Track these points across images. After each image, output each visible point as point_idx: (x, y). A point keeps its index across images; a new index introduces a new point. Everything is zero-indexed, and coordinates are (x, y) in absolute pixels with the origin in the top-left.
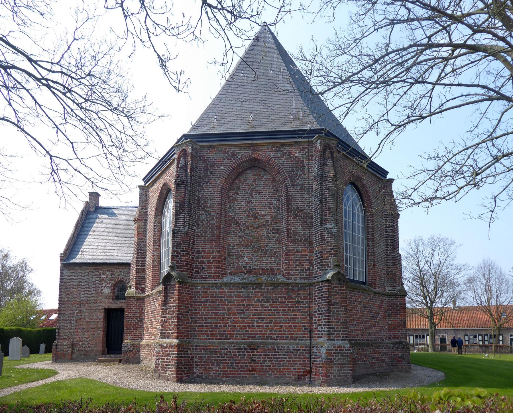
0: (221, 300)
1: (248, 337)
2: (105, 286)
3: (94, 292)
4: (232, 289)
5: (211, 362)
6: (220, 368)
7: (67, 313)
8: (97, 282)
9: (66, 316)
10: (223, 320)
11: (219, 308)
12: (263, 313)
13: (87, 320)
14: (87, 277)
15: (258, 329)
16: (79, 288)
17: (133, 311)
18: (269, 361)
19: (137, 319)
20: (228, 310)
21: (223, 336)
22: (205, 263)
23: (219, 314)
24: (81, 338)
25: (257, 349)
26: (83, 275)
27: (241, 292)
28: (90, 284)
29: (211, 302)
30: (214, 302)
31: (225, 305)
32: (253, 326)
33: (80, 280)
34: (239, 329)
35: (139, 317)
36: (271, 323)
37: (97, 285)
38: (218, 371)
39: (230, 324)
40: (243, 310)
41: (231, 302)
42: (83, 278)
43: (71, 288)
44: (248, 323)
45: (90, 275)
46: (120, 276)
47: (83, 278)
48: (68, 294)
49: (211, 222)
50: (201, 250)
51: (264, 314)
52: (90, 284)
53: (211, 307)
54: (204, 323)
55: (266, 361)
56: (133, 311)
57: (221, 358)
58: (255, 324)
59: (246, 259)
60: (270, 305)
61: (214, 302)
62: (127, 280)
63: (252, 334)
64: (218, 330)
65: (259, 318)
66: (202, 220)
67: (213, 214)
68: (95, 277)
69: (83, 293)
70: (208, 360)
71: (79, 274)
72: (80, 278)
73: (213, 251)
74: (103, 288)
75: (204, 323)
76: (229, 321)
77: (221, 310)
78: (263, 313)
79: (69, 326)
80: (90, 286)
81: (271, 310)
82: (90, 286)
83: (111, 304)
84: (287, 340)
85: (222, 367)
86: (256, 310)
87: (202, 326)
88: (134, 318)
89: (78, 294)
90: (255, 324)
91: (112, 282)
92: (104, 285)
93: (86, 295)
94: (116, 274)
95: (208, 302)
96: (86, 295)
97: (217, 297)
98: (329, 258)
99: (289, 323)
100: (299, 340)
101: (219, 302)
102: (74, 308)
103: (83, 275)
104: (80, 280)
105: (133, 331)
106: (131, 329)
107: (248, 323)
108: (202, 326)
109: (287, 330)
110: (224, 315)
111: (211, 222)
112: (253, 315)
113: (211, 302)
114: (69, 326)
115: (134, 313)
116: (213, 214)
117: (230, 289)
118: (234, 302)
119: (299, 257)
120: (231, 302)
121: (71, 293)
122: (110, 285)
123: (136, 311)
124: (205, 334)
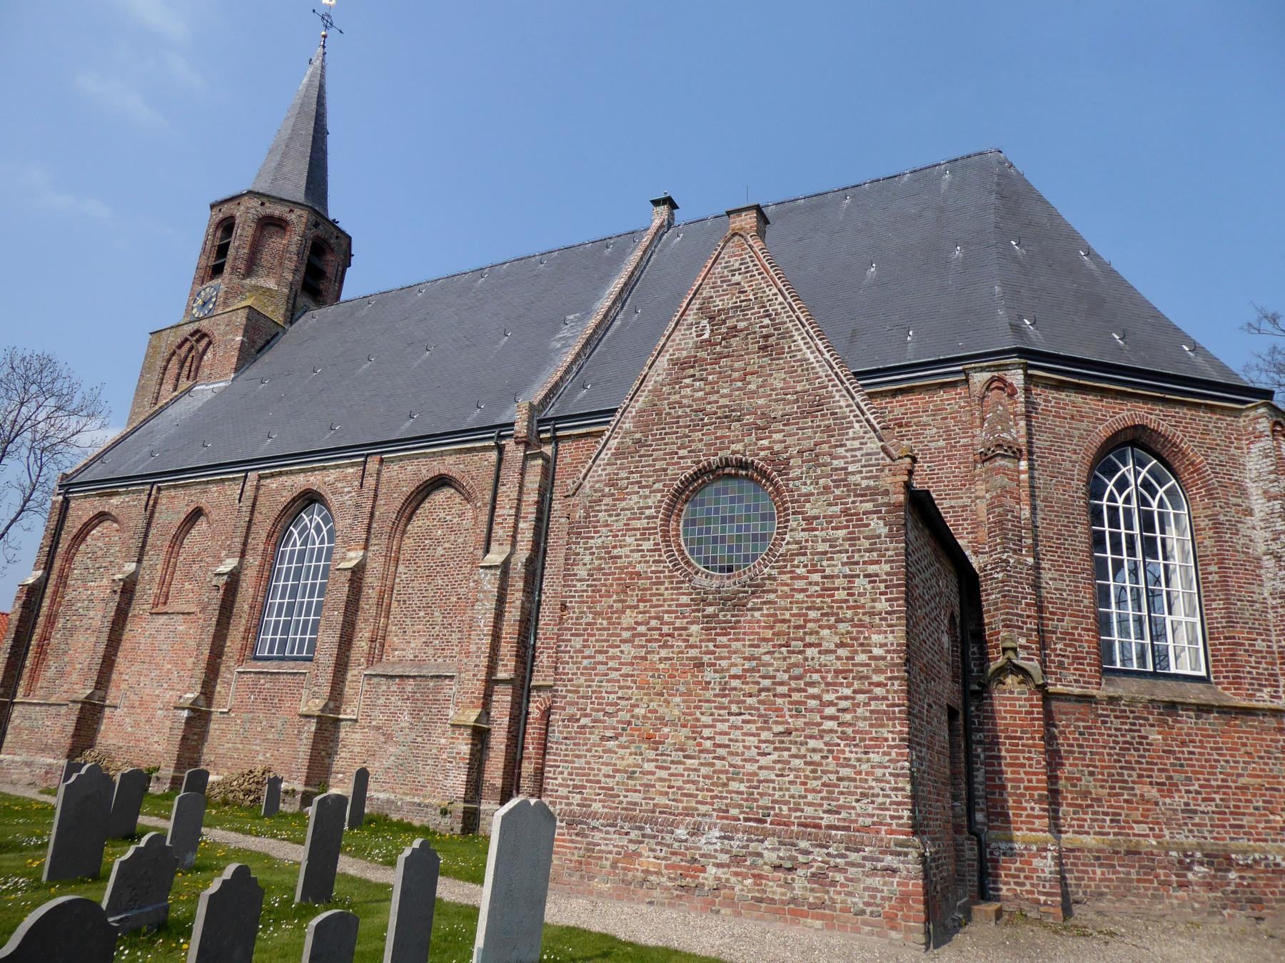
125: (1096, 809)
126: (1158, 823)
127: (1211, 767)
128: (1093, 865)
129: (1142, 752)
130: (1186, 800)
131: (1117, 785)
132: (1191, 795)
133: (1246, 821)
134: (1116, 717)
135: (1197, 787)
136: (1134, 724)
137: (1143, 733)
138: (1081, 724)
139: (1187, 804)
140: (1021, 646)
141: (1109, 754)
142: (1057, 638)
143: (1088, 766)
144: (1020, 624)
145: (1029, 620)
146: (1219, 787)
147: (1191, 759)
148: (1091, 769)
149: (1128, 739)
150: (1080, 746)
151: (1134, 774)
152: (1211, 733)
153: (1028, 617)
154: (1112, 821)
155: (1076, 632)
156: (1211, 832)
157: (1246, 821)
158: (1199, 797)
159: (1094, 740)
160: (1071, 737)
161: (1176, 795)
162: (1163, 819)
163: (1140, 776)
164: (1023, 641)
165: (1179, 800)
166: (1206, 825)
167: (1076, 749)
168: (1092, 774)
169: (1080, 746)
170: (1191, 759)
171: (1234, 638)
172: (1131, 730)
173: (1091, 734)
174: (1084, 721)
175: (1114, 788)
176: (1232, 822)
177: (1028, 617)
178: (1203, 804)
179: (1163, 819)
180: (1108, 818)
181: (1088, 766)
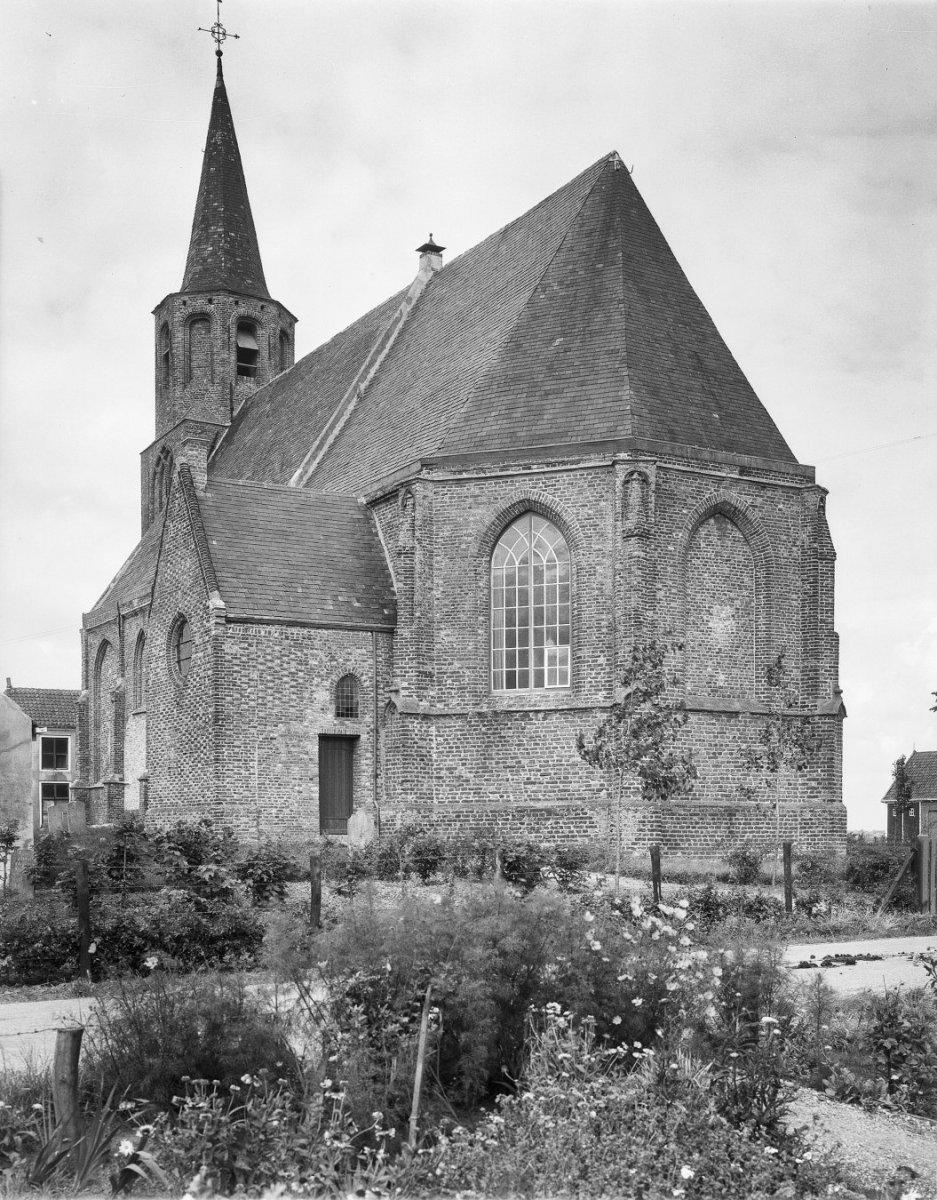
1: (722, 795)
2: (317, 686)
3: (294, 697)
6: (690, 845)
7: (236, 743)
8: (301, 674)
9: (236, 750)
13: (283, 759)
18: (751, 832)
19: (423, 760)
25: (735, 815)
26: (269, 657)
27: (713, 724)
28: (285, 679)
32: (728, 778)
33: (261, 667)
37: (301, 681)
38: (687, 848)
40: (714, 753)
42: (269, 664)
43: (244, 685)
45: (285, 658)
46: (350, 665)
47: (269, 664)
48: (237, 699)
52: (285, 679)
55: (746, 832)
68: (293, 664)
70: (675, 832)
72: (261, 664)
74: (314, 688)
79: (242, 771)
80: (286, 683)
82: (286, 683)
83: (329, 723)
85: (692, 842)
89: (260, 701)
91: (333, 677)
92: (315, 682)
96: (277, 702)
103: (269, 657)
104: (261, 667)
114: (242, 771)
115: (418, 747)
121: (242, 696)
122: (327, 684)
123: (421, 743)
126: (506, 792)
127: (550, 752)
128: (455, 821)
129: (500, 748)
131: (480, 770)
133: (571, 787)
134: (484, 726)
135: (538, 767)
136: (497, 729)
137: (502, 734)
138: (459, 733)
139: (528, 779)
140: (403, 688)
141: (478, 751)
143: (461, 760)
146: (554, 765)
148: (464, 761)
149: (492, 739)
150: (457, 747)
151: (493, 762)
152: (552, 729)
155: (461, 671)
156: (544, 795)
157: (571, 787)
161: (522, 773)
162: (510, 789)
163: (497, 763)
164: (405, 684)
165: (524, 775)
166: (541, 791)
167: (454, 749)
168: (464, 764)
169: (457, 747)
171: (580, 657)
172: (494, 734)
173: (465, 739)
175: (477, 772)
176: (561, 787)
179: (510, 789)
181: (461, 760)
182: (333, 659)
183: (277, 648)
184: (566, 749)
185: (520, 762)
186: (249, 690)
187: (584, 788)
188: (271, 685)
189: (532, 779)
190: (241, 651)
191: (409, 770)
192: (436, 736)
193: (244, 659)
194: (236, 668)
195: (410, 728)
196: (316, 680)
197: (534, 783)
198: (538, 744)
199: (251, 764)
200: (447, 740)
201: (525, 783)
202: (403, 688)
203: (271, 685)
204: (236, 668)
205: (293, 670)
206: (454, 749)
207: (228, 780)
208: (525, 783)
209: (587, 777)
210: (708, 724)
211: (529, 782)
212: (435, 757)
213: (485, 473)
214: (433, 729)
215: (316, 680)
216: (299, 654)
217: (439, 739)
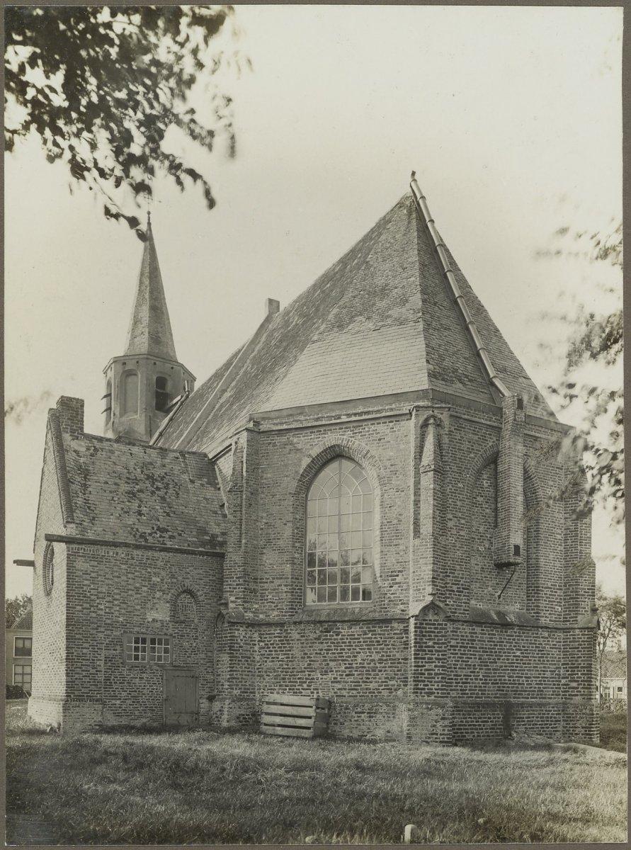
0: (472, 644)
4: (484, 630)
5: (464, 729)
9: (85, 651)
10: (474, 672)
11: (471, 654)
12: (514, 663)
14: (124, 578)
15: (510, 684)
16: (108, 599)
17: (240, 647)
19: (247, 661)
20: (480, 659)
21: (474, 694)
22: (454, 591)
23: (469, 663)
24: (117, 693)
28: (130, 592)
29: (461, 647)
30: (464, 647)
31: (477, 652)
34: (490, 685)
35: (250, 658)
36: (522, 677)
39: (481, 677)
40: (494, 659)
41: (482, 648)
42: (116, 580)
44: (500, 676)
45: (130, 575)
49: (462, 533)
50: (449, 571)
51: (516, 664)
52: (130, 592)
53: (461, 654)
54: (454, 675)
56: (240, 647)
57: (475, 723)
58: (507, 678)
59: (490, 589)
60: (522, 653)
61: (464, 647)
62: (198, 590)
63: (503, 691)
64: (468, 685)
65: (511, 670)
66: (451, 528)
67: (463, 521)
69: (118, 608)
71: (107, 570)
73: (463, 574)
75: (454, 675)
76: (480, 674)
77: (471, 658)
78: (514, 663)
81: (522, 660)
84: (537, 698)
86: (508, 660)
87: (452, 679)
88: (243, 660)
90: (507, 678)
91: (172, 591)
93: (123, 611)
94: (180, 578)
95: (457, 647)
96: (123, 611)
97: (468, 640)
98: (587, 600)
99: (539, 677)
100: (549, 698)
101: (470, 647)
102: (100, 635)
105: (241, 682)
106: (238, 679)
107: (500, 676)
108: (452, 679)
109: (537, 686)
110: (474, 665)
111: (462, 533)
112: (505, 667)
113: (461, 647)
116: (463, 521)
117: (482, 630)
118: (486, 648)
119: (550, 595)
120: (482, 648)
124: (454, 690)
125: (282, 683)
130: (335, 676)
132: (338, 673)
139: (334, 678)
140: (232, 602)
142: (269, 593)
144: (232, 590)
145: (238, 587)
147: (342, 653)
152: (356, 636)
153: (237, 585)
154: (290, 689)
156: (349, 693)
158: (344, 674)
159: (284, 647)
160: (271, 646)
164: (233, 598)
167: (273, 653)
170: (342, 653)
174: (279, 637)
177: (237, 585)
178: (346, 678)
180: (287, 688)
182: (173, 577)
183: (123, 566)
184: (368, 654)
185: (328, 664)
186: (98, 601)
187: (383, 687)
188: (118, 597)
189: (339, 679)
190: (91, 569)
191: (234, 669)
192: (259, 641)
193: (93, 575)
194: (86, 582)
195: (236, 634)
196: (158, 594)
197: (339, 682)
198: (344, 650)
199: (98, 663)
200: (267, 644)
201: (332, 682)
202: (232, 602)
203: (118, 597)
204: (86, 582)
205: (138, 585)
206: (273, 653)
207: (77, 676)
208: (332, 682)
209: (386, 678)
210: (489, 634)
211: (335, 681)
212: (258, 658)
213: (302, 423)
214: (256, 635)
215: (158, 594)
216: (143, 572)
217: (261, 644)
